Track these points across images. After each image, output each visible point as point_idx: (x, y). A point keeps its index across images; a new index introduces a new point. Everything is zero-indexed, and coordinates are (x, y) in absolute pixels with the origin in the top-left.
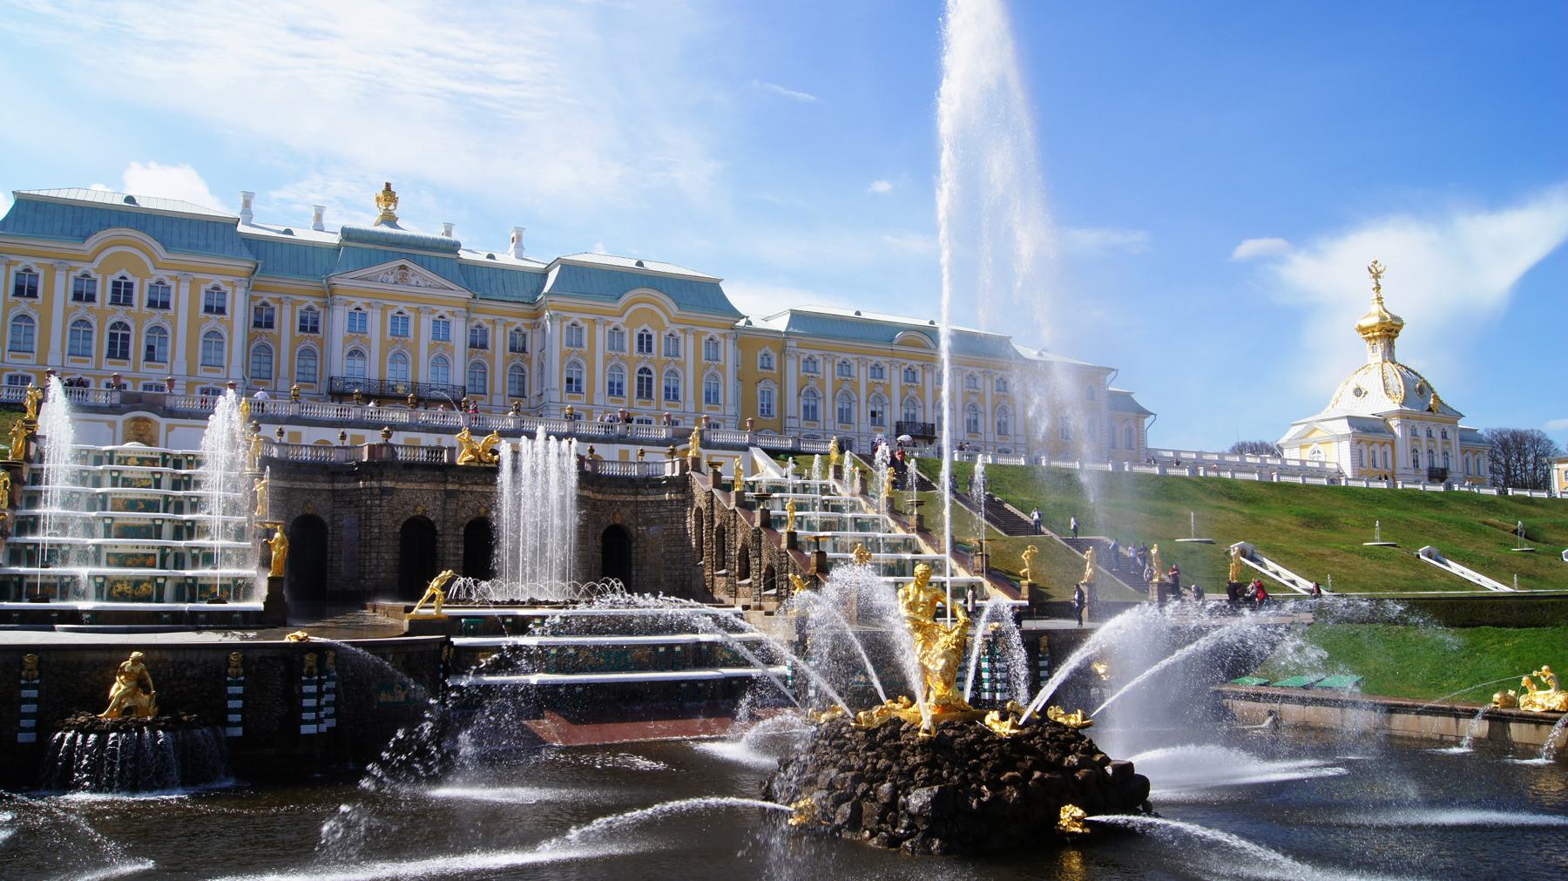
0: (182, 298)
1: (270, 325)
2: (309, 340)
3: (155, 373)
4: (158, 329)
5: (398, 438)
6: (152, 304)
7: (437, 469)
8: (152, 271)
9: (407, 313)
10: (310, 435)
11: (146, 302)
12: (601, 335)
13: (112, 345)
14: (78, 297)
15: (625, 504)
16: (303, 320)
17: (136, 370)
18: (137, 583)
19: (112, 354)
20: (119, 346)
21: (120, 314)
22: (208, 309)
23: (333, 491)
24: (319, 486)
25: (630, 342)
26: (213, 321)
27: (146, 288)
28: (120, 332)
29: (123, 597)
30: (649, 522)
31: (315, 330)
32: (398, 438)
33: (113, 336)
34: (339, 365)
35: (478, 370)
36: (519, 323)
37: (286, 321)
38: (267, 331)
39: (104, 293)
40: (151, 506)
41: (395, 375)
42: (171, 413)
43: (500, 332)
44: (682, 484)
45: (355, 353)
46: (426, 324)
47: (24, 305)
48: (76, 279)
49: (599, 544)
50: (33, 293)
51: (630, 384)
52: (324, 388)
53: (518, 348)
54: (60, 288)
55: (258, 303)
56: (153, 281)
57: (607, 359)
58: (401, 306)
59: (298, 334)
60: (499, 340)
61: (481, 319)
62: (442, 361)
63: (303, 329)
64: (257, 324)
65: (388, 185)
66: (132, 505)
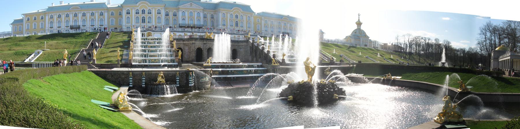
0: (153, 12)
2: (175, 17)
3: (150, 25)
4: (150, 17)
6: (148, 13)
7: (202, 39)
10: (178, 34)
12: (228, 15)
14: (136, 13)
18: (155, 60)
21: (143, 15)
25: (234, 17)
26: (159, 15)
29: (153, 62)
30: (241, 48)
34: (181, 22)
35: (205, 21)
36: (212, 13)
37: (171, 14)
39: (140, 12)
40: (155, 47)
41: (191, 23)
42: (154, 31)
44: (247, 41)
45: (184, 19)
46: (196, 14)
50: (129, 13)
51: (234, 24)
52: (178, 26)
53: (212, 17)
57: (230, 20)
60: (209, 16)
61: (205, 12)
62: (199, 20)
66: (151, 47)
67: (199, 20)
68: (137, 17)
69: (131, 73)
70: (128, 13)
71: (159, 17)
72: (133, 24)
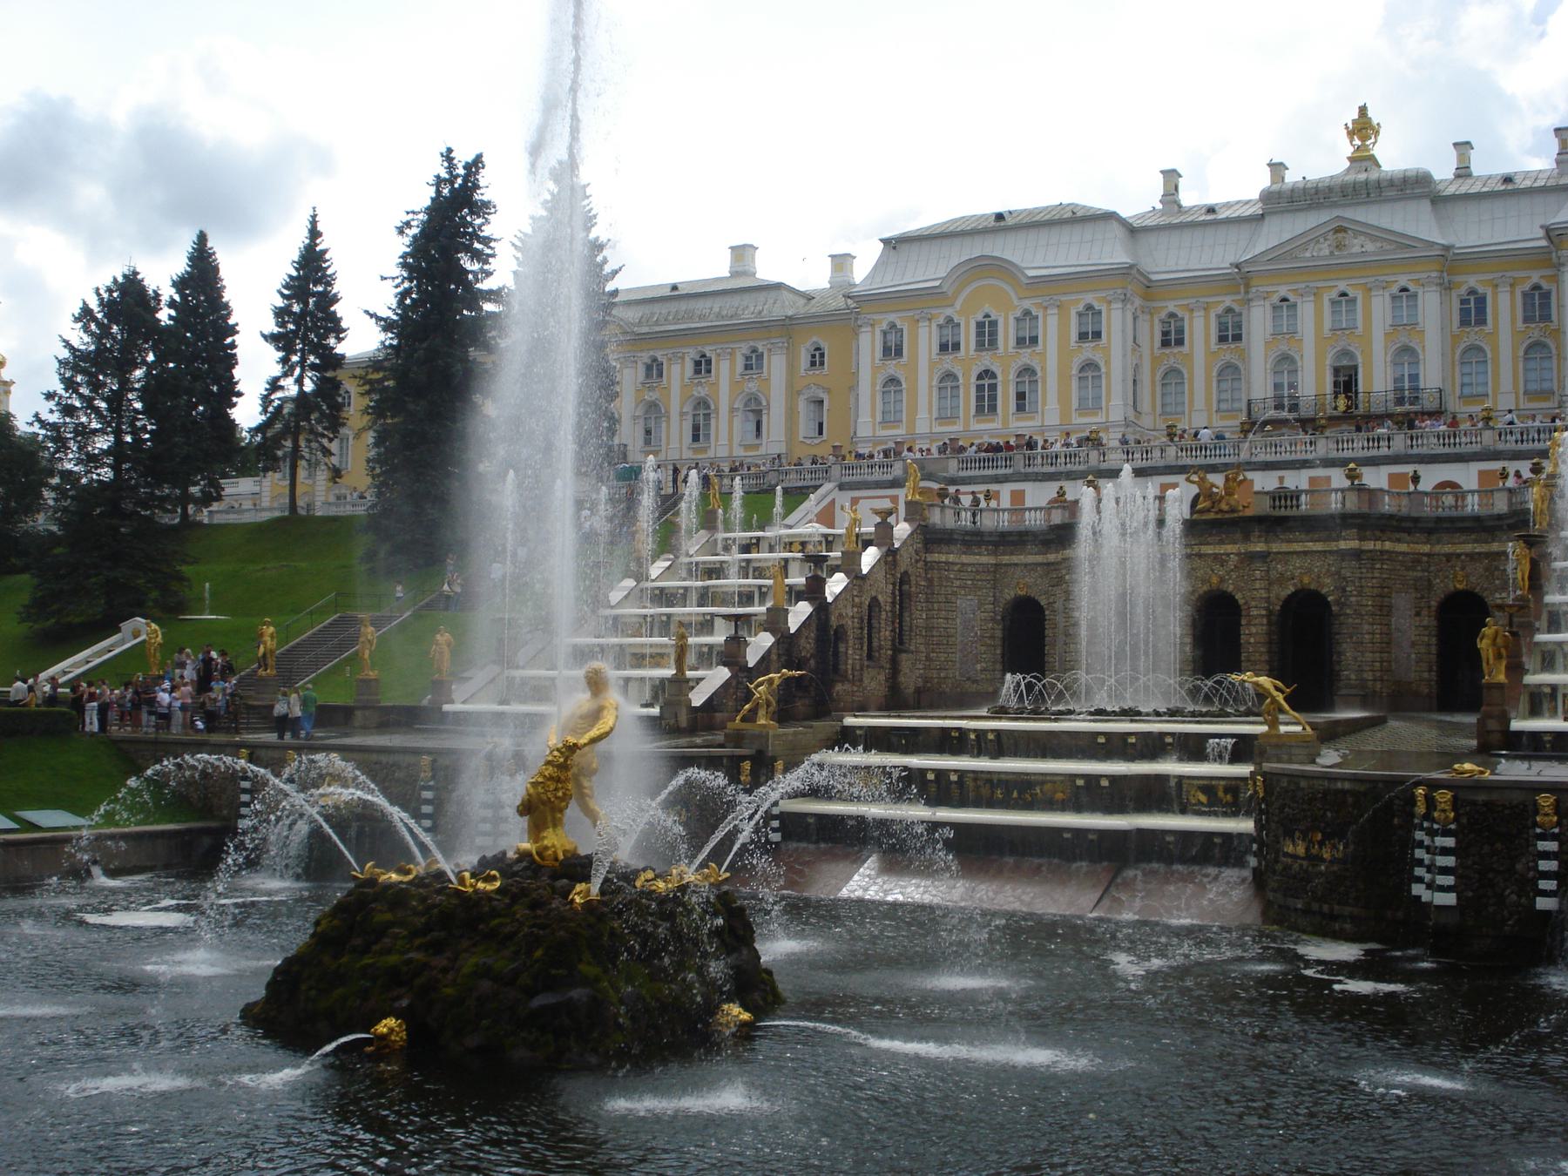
0: (1050, 329)
1: (1180, 342)
2: (1228, 353)
3: (1024, 426)
4: (1027, 371)
5: (1376, 478)
6: (1020, 342)
8: (1016, 302)
11: (1012, 342)
13: (980, 398)
14: (943, 348)
15: (1472, 557)
16: (1222, 327)
17: (1005, 422)
19: (980, 409)
20: (986, 402)
21: (987, 361)
22: (1083, 336)
23: (1048, 564)
24: (1031, 559)
26: (1088, 351)
27: (1012, 322)
28: (986, 382)
31: (1237, 338)
33: (980, 388)
34: (1260, 385)
36: (1535, 277)
37: (1200, 331)
38: (1176, 350)
39: (968, 337)
43: (1504, 299)
45: (1286, 362)
47: (892, 367)
48: (940, 327)
49: (1428, 620)
50: (899, 352)
54: (924, 341)
55: (1163, 315)
56: (1018, 314)
58: (1342, 286)
59: (1214, 346)
61: (1472, 281)
62: (1407, 353)
63: (1222, 339)
64: (1165, 343)
65: (1363, 110)
67: (1407, 353)
68: (949, 376)
70: (892, 351)
71: (1089, 366)
72: (922, 427)
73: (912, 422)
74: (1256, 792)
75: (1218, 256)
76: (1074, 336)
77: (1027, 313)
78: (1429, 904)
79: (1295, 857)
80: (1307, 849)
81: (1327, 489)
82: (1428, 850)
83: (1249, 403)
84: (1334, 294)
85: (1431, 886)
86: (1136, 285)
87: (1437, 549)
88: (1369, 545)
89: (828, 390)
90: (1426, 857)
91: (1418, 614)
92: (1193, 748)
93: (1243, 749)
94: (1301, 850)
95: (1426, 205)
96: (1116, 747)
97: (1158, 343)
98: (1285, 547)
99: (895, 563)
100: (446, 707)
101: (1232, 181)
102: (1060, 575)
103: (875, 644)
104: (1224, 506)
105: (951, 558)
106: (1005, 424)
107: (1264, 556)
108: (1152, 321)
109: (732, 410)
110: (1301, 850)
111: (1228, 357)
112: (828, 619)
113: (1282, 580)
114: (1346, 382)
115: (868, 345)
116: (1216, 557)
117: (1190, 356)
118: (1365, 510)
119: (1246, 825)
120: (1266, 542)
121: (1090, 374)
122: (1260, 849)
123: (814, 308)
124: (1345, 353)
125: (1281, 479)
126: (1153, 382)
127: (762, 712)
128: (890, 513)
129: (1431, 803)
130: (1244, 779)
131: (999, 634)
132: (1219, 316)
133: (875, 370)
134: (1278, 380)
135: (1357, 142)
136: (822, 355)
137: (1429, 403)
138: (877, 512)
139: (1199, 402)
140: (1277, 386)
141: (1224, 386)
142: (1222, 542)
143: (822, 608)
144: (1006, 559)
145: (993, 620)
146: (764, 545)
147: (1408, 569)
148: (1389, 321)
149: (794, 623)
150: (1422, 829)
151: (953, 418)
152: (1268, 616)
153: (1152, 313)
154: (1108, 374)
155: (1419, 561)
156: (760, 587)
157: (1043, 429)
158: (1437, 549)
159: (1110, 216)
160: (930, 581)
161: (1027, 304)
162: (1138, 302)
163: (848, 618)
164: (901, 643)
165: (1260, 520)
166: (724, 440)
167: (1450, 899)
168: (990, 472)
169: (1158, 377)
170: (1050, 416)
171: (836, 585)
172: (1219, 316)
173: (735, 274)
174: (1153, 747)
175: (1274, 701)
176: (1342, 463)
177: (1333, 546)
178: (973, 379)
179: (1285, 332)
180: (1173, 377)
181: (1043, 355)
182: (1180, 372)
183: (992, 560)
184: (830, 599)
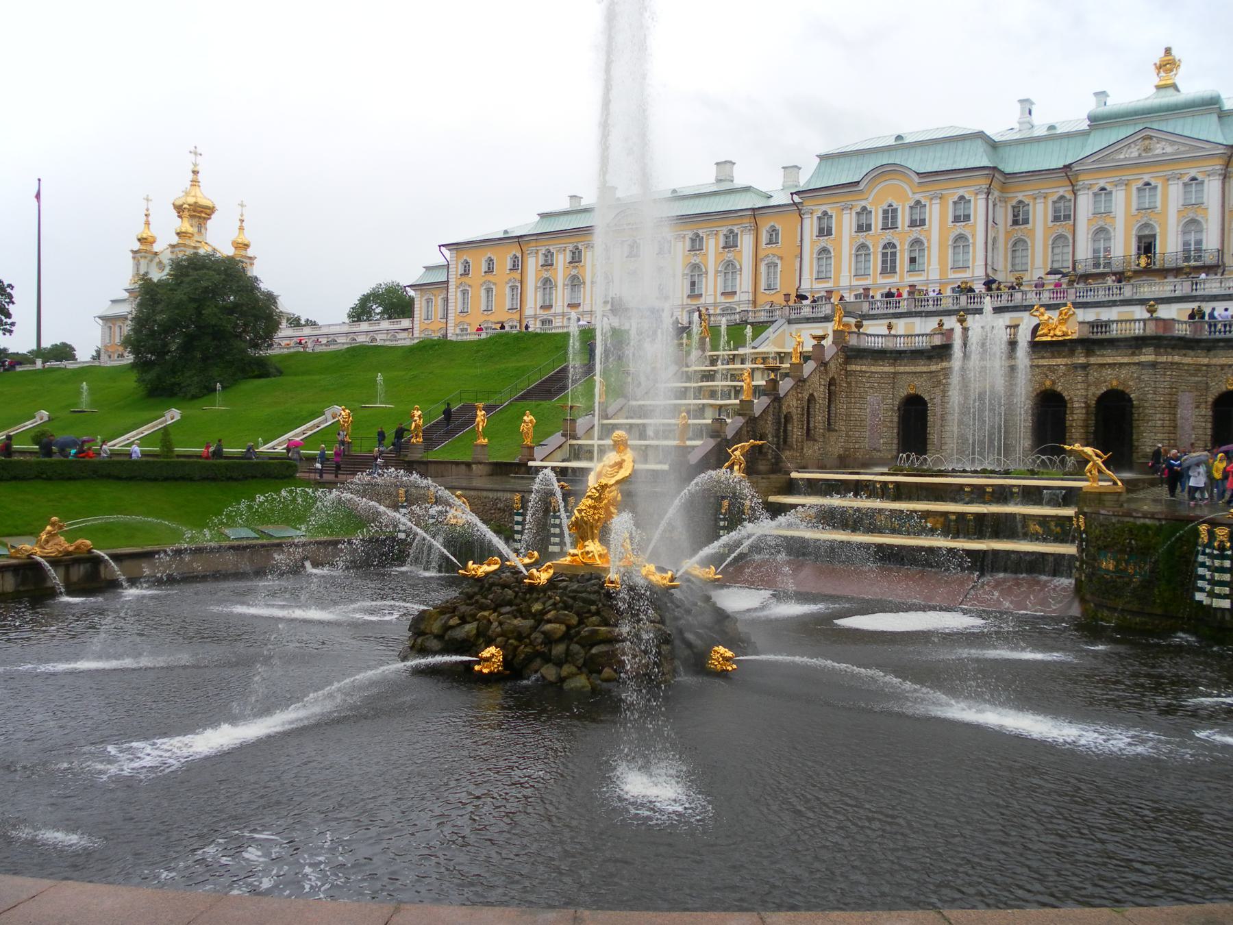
1: (1026, 221)
2: (1063, 228)
4: (917, 242)
6: (913, 224)
9: (1153, 183)
11: (907, 223)
13: (884, 262)
14: (860, 229)
16: (1056, 210)
19: (884, 271)
21: (889, 236)
22: (957, 219)
24: (918, 369)
26: (960, 228)
28: (889, 251)
32: (871, 327)
37: (1040, 213)
39: (877, 221)
45: (1101, 233)
46: (1175, 191)
47: (824, 242)
48: (858, 213)
50: (829, 233)
54: (846, 224)
55: (1014, 202)
58: (1146, 178)
59: (1050, 224)
62: (1192, 224)
63: (1056, 219)
64: (1015, 222)
65: (1168, 51)
67: (1192, 224)
68: (863, 246)
69: (402, 491)
70: (825, 231)
71: (961, 238)
73: (837, 279)
74: (1079, 527)
75: (1054, 159)
76: (950, 218)
77: (918, 202)
78: (1210, 606)
79: (1107, 571)
80: (1116, 567)
81: (1127, 319)
82: (1209, 568)
83: (1074, 263)
84: (1140, 184)
85: (1212, 594)
86: (998, 180)
87: (1215, 361)
88: (1163, 359)
89: (781, 258)
90: (1208, 574)
91: (1198, 407)
92: (1032, 495)
93: (1069, 497)
94: (1111, 567)
95: (1215, 118)
96: (979, 494)
97: (1010, 222)
98: (1100, 360)
99: (826, 372)
100: (531, 463)
101: (1066, 108)
102: (940, 381)
103: (812, 425)
104: (1059, 333)
105: (864, 368)
106: (902, 279)
107: (1085, 367)
108: (1006, 207)
109: (717, 272)
110: (1111, 567)
111: (1060, 231)
112: (780, 407)
113: (1097, 383)
114: (1147, 246)
115: (810, 226)
116: (1050, 367)
117: (1033, 230)
118: (1160, 333)
119: (1070, 549)
120: (1087, 355)
121: (961, 244)
122: (1081, 565)
123: (772, 202)
124: (1146, 225)
125: (1098, 314)
126: (1006, 249)
127: (736, 467)
128: (823, 338)
129: (1212, 535)
130: (1069, 518)
131: (896, 419)
132: (1054, 202)
133: (813, 243)
134: (1096, 246)
135: (1162, 74)
136: (777, 235)
137: (1209, 259)
138: (814, 337)
139: (1039, 261)
140: (1096, 251)
141: (1057, 251)
142: (1053, 357)
143: (777, 399)
144: (902, 369)
145: (892, 410)
146: (738, 360)
147: (1191, 375)
148: (1181, 202)
149: (757, 412)
150: (1204, 553)
151: (866, 275)
152: (1087, 407)
153: (1005, 201)
154: (974, 244)
155: (1200, 370)
156: (735, 387)
157: (928, 282)
158: (1215, 361)
159: (981, 136)
160: (849, 383)
161: (918, 197)
162: (996, 194)
163: (792, 405)
164: (829, 424)
165: (1081, 342)
166: (711, 291)
167: (1226, 604)
168: (891, 311)
169: (1010, 246)
170: (934, 273)
171: (785, 385)
172: (1054, 202)
173: (719, 181)
174: (1002, 495)
175: (1095, 464)
176: (1142, 302)
177: (1136, 359)
178: (880, 249)
179: (1102, 215)
180: (1018, 245)
181: (929, 230)
182: (1025, 242)
183: (892, 370)
184: (782, 394)
